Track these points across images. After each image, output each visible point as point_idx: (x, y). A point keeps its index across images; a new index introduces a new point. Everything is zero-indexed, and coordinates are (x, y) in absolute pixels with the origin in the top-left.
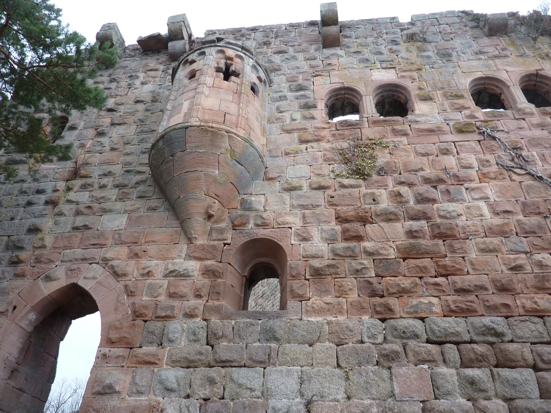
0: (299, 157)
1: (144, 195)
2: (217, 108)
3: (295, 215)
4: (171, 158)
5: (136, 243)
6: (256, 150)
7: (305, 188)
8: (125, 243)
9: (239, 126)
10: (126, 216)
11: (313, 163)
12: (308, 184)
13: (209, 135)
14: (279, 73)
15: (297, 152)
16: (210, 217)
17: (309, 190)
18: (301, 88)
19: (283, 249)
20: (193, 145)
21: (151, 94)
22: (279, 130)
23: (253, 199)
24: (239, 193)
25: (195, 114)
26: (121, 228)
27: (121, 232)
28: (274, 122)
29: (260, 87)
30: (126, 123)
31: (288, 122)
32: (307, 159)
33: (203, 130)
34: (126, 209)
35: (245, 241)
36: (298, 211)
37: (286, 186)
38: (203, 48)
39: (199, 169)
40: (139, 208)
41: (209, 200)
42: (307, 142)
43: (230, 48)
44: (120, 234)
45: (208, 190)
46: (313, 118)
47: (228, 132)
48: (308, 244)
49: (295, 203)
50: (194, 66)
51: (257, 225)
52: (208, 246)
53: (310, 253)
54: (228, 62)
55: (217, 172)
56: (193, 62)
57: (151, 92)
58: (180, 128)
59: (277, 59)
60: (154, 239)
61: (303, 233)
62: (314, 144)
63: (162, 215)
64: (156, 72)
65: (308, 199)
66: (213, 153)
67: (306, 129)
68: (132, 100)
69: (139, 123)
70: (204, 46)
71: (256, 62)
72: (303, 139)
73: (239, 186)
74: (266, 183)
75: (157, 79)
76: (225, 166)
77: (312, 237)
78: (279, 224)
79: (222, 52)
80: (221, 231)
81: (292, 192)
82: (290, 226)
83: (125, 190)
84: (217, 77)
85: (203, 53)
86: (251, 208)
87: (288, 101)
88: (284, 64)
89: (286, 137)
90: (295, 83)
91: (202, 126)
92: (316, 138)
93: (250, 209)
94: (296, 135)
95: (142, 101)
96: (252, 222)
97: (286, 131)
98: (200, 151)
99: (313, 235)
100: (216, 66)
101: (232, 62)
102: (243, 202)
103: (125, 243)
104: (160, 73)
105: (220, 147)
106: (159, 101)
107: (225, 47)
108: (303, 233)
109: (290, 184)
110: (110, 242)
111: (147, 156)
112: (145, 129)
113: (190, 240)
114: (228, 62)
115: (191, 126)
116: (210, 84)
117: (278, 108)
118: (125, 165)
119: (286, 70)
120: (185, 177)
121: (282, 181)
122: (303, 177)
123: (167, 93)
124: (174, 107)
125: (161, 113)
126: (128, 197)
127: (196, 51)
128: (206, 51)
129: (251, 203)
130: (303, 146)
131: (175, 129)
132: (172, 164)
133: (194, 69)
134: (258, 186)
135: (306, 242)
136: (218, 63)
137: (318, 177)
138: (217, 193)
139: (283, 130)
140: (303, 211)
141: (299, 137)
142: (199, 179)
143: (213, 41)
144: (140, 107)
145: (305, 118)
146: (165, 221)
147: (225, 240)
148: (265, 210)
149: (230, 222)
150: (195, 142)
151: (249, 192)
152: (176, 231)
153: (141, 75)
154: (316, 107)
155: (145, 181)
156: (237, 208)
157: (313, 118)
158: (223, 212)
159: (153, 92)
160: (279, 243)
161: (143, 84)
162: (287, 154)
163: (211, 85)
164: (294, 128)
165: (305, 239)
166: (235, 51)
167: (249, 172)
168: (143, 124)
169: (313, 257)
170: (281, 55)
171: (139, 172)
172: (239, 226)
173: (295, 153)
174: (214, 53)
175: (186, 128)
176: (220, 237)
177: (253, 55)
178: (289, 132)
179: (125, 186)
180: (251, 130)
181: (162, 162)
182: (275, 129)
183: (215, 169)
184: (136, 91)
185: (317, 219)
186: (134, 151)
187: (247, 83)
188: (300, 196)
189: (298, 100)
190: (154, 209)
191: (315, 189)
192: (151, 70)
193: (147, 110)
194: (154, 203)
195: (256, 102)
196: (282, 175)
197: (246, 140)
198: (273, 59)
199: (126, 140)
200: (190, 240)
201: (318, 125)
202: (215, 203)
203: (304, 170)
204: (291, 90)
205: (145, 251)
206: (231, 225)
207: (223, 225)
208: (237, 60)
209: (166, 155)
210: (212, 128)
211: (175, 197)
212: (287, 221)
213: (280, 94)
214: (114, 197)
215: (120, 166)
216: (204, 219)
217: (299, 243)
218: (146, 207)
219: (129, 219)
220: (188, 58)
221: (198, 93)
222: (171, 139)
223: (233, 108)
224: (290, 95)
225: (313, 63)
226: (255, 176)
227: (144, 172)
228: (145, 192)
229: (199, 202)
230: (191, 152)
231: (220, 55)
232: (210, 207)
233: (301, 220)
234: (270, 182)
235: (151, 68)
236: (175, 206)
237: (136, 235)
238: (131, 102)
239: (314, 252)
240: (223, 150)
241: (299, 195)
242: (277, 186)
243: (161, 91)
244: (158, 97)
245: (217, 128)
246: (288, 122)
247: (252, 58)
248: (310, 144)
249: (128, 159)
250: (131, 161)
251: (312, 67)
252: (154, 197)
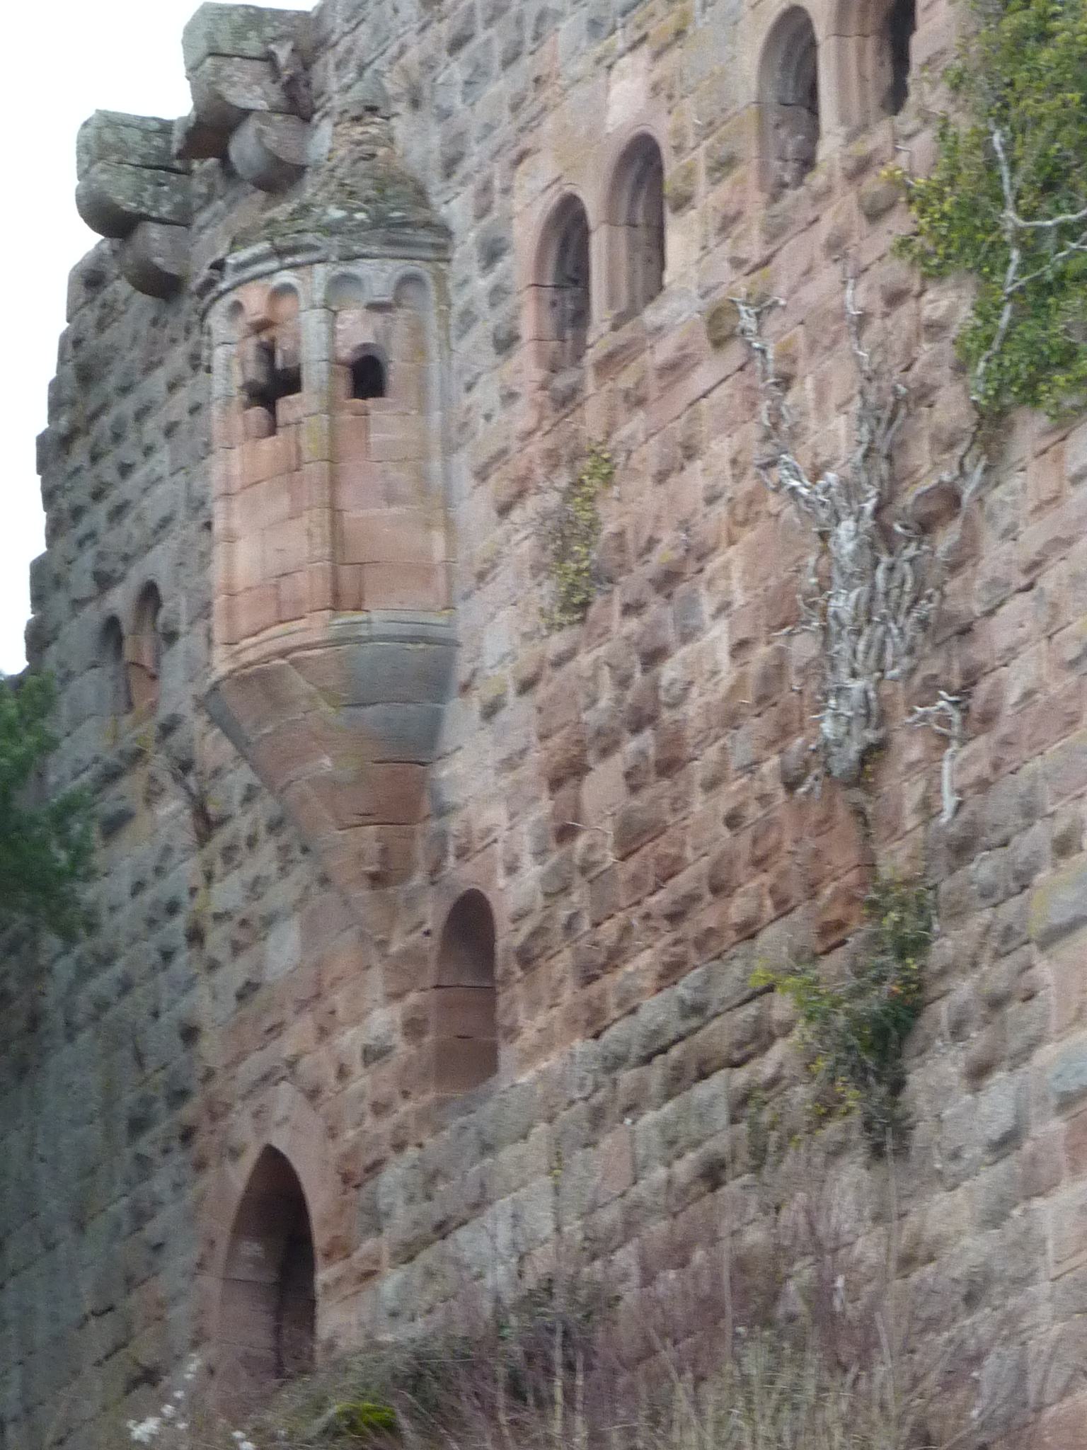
39: (292, 774)
47: (283, 654)
98: (266, 731)
114: (264, 338)
138: (363, 811)
167: (407, 701)
210: (250, 664)
247: (319, 262)
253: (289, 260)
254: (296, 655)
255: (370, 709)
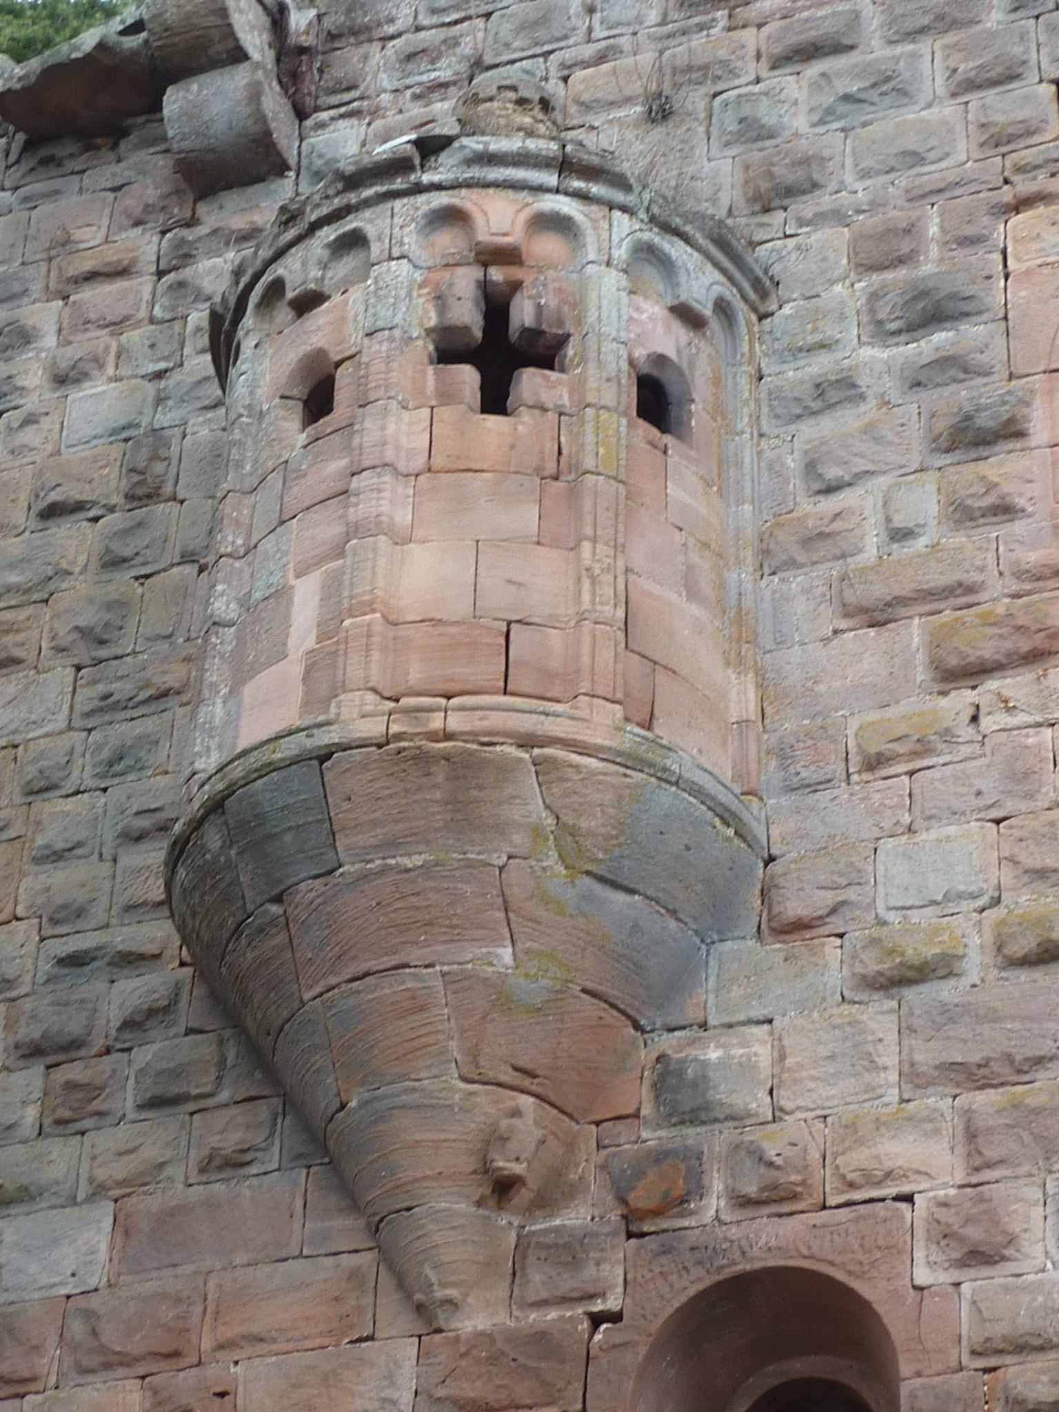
0: (938, 778)
1: (174, 1090)
2: (459, 607)
3: (929, 1124)
4: (275, 909)
5: (176, 1354)
6: (698, 792)
7: (976, 962)
8: (124, 1361)
9: (585, 687)
10: (104, 1212)
11: (1010, 806)
12: (989, 937)
13: (440, 778)
14: (806, 207)
15: (924, 748)
16: (504, 1188)
17: (994, 972)
18: (932, 311)
19: (876, 1316)
20: (368, 838)
21: (116, 451)
22: (827, 611)
23: (713, 1054)
24: (637, 1027)
25: (354, 669)
26: (92, 1282)
27: (95, 1302)
28: (792, 564)
29: (698, 363)
30: (16, 661)
31: (871, 544)
32: (979, 784)
33: (405, 757)
34: (101, 1174)
35: (692, 1292)
36: (937, 1101)
37: (872, 964)
38: (347, 210)
39: (416, 955)
40: (161, 1166)
41: (487, 1104)
42: (973, 672)
43: (496, 185)
44: (89, 1315)
45: (474, 1054)
46: (1005, 510)
47: (527, 742)
48: (999, 1275)
49: (926, 1055)
50: (317, 331)
51: (744, 1202)
52: (511, 1337)
53: (999, 1330)
54: (497, 274)
55: (506, 954)
56: (308, 302)
57: (114, 432)
58: (295, 761)
59: (793, 102)
60: (255, 1328)
61: (968, 1221)
62: (1015, 685)
63: (275, 1189)
64: (121, 284)
65: (986, 1029)
66: (470, 864)
67: (970, 589)
68: (23, 498)
69: (83, 653)
70: (352, 198)
71: (653, 219)
72: (953, 662)
73: (639, 996)
74: (775, 949)
75: (135, 337)
76: (542, 914)
77: (1012, 1240)
78: (852, 1185)
79: (453, 217)
80: (569, 1251)
81: (910, 993)
82: (906, 1189)
83: (74, 1072)
84: (446, 396)
85: (355, 240)
86: (707, 1107)
87: (869, 409)
88: (831, 140)
89: (865, 652)
90: (902, 273)
91: (399, 737)
92: (1025, 646)
93: (699, 1114)
94: (914, 632)
95: (79, 507)
96: (717, 1184)
97: (863, 610)
98: (407, 862)
99: (1016, 1227)
100: (433, 321)
101: (515, 273)
102: (667, 1077)
103: (124, 1361)
104: (143, 285)
105: (500, 829)
106: (168, 489)
107: (468, 184)
108: (968, 1221)
109: (891, 952)
110: (49, 1361)
111: (154, 854)
112: (122, 689)
113: (428, 1316)
114: (497, 274)
115: (345, 748)
116: (411, 454)
117: (811, 468)
118: (54, 922)
119: (849, 178)
120: (352, 1002)
121: (854, 936)
122: (961, 896)
123: (202, 429)
124: (245, 603)
125: (190, 570)
126: (96, 1105)
127: (315, 226)
128: (370, 231)
129: (702, 1082)
130: (962, 699)
131: (271, 768)
132: (282, 938)
133: (320, 354)
134: (739, 971)
135: (985, 1271)
136: (440, 299)
137: (1039, 886)
138: (523, 1062)
139: (848, 612)
140: (964, 1099)
141: (935, 642)
142: (422, 1008)
143: (398, 165)
144: (75, 542)
145: (962, 514)
146: (297, 1225)
147: (591, 1297)
148: (779, 1113)
149: (610, 1199)
150: (375, 823)
151: (694, 1015)
152: (355, 1275)
153: (44, 316)
154: (1020, 434)
155: (166, 1010)
156: (636, 1115)
157: (1005, 510)
158: (571, 1145)
159: (123, 433)
160: (855, 1284)
161: (63, 379)
162: (873, 763)
163: (420, 462)
164: (903, 588)
165: (979, 1257)
166: (524, 196)
167: (673, 913)
168: (103, 653)
169: (1021, 1347)
170: (814, 69)
171: (131, 960)
172: (657, 1213)
173: (915, 754)
174: (411, 240)
175: (324, 756)
176: (568, 1284)
177: (628, 188)
178: (877, 617)
179: (72, 1046)
180: (661, 676)
181: (237, 931)
182: (801, 605)
183: (497, 941)
184: (29, 436)
185: (1038, 1138)
186: (82, 834)
187: (609, 398)
188: (948, 1014)
189: (924, 395)
190: (230, 1164)
191: (1026, 962)
192: (92, 277)
193: (113, 562)
194: (228, 1129)
195: (683, 482)
196: (851, 894)
197: (630, 761)
198: (767, 115)
199: (31, 771)
200: (428, 1316)
201: (1033, 557)
202: (516, 1113)
203: (960, 854)
204: (882, 333)
205: (222, 1395)
206: (614, 1216)
207: (575, 1217)
208: (548, 246)
209: (249, 895)
210: (449, 736)
211: (324, 1101)
212: (888, 1164)
213: (819, 365)
214: (31, 1114)
215: (25, 931)
216: (479, 1204)
217: (954, 1275)
218: (195, 1156)
219: (123, 1227)
220: (279, 270)
221: (354, 530)
222: (261, 818)
223: (545, 583)
224: (875, 360)
225: (1001, 106)
226: (716, 919)
227: (156, 957)
228: (176, 1073)
229: (444, 1114)
230: (365, 877)
231: (448, 240)
232: (495, 1138)
233: (960, 1149)
234: (796, 945)
235: (88, 266)
236: (331, 1144)
237: (167, 1313)
238: (19, 516)
239: (1024, 1323)
240: (517, 838)
241: (944, 1009)
242: (833, 964)
243: (164, 418)
244: (159, 467)
245: (472, 736)
246: (870, 553)
247: (624, 209)
248: (992, 684)
249: (64, 881)
250: (80, 896)
251: (999, 140)
252: (224, 1096)
253: (577, 184)
254: (548, 751)
255: (621, 897)
